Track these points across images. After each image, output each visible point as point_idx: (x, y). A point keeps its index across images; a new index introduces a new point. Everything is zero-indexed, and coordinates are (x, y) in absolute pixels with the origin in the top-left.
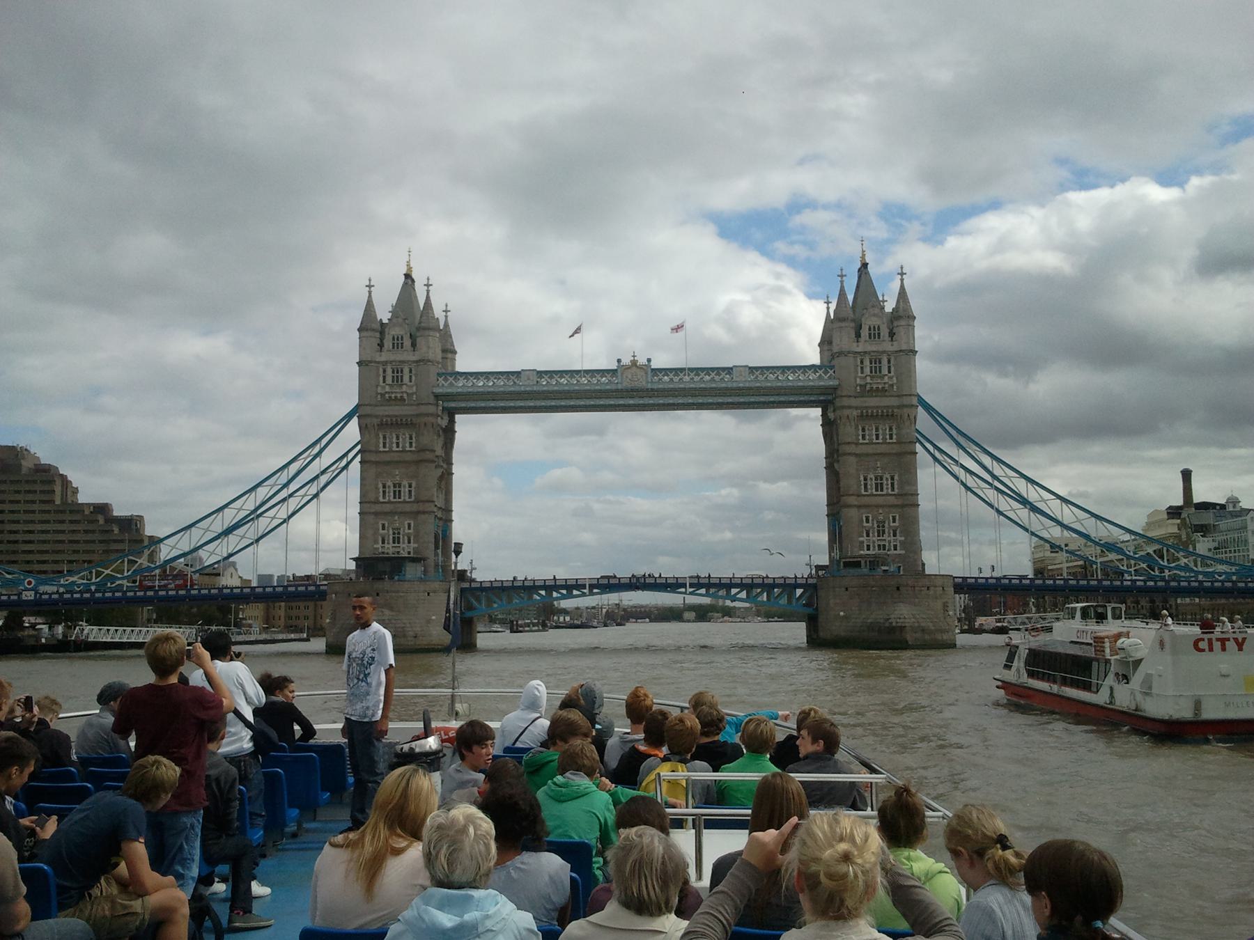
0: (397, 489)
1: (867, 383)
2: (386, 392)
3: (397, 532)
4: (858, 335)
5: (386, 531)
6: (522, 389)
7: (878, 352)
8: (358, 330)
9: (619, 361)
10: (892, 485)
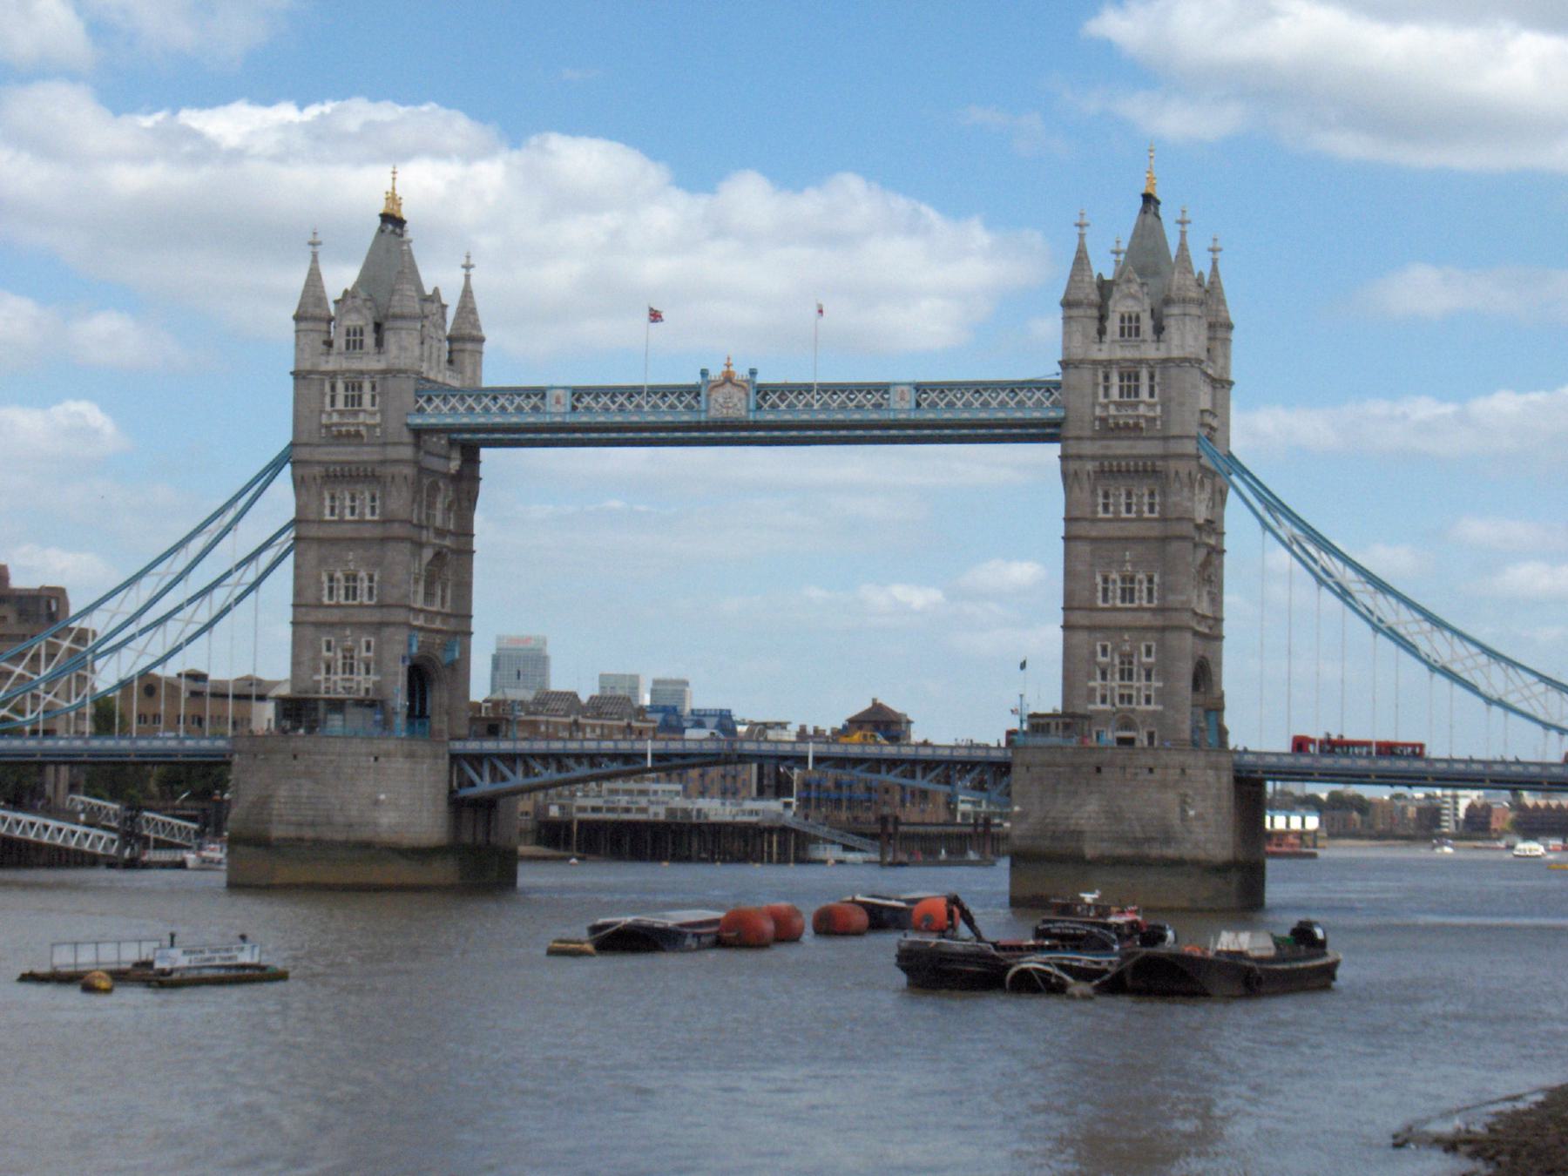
0: (351, 584)
1: (1109, 416)
2: (332, 425)
3: (349, 655)
4: (1102, 332)
5: (331, 654)
6: (548, 419)
7: (1131, 361)
8: (298, 318)
9: (704, 373)
10: (1150, 591)
